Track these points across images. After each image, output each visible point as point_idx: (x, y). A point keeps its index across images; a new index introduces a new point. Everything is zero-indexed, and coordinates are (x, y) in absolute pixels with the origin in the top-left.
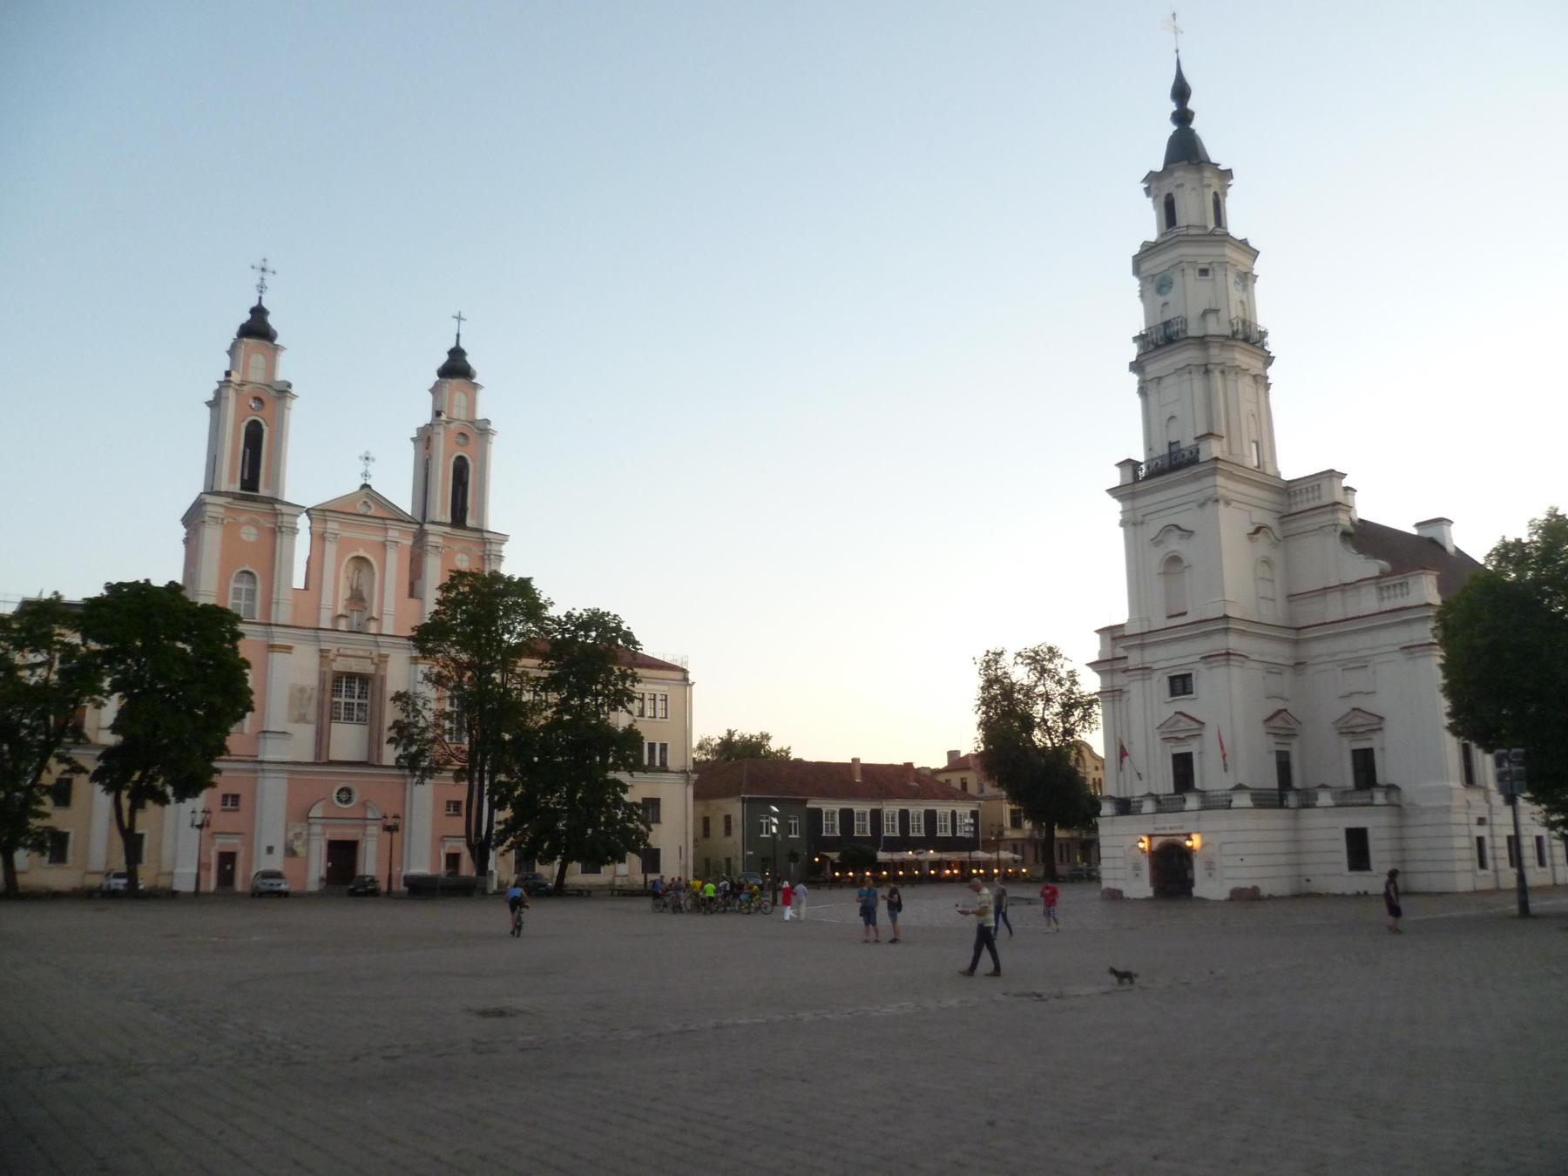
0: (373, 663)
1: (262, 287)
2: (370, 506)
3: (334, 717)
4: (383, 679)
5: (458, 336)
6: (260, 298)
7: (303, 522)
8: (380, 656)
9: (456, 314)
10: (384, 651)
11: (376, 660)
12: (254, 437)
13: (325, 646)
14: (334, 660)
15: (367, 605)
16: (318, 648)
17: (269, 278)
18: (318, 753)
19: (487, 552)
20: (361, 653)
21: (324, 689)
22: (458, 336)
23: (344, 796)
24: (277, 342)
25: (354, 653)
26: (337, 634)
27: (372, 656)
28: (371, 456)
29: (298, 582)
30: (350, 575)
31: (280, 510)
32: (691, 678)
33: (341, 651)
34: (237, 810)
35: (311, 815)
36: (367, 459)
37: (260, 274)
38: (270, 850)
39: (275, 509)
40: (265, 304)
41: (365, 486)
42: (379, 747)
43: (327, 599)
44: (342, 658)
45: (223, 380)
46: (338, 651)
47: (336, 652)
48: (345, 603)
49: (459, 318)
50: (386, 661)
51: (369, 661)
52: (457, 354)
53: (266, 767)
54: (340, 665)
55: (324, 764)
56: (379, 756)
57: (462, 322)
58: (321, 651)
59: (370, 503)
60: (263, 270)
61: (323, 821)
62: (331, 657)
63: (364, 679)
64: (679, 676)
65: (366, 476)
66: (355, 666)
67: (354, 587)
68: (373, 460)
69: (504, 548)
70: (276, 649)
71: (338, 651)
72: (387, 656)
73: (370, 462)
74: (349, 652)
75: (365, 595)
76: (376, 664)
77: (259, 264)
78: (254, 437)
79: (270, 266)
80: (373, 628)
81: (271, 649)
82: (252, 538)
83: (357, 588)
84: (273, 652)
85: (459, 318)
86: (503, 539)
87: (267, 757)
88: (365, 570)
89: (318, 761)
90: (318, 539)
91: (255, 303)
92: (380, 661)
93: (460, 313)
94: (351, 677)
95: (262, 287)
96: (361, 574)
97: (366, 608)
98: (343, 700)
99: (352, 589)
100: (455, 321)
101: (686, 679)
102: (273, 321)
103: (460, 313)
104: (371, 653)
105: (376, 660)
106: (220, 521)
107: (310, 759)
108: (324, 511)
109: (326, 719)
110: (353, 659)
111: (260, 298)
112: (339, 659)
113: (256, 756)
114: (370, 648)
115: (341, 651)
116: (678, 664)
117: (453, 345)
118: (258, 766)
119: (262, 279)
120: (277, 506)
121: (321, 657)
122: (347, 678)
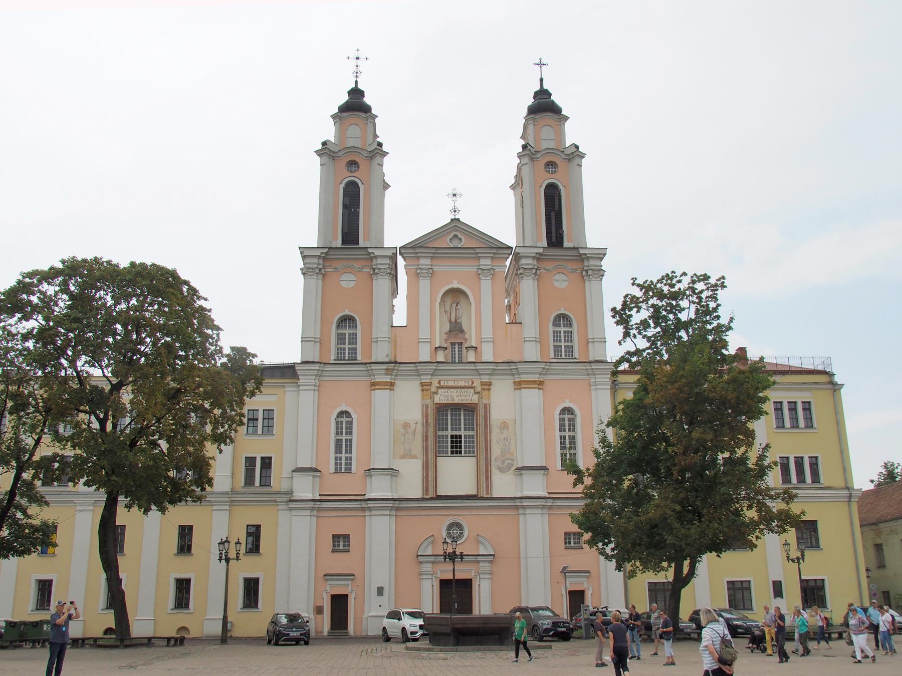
0: (476, 393)
1: (357, 73)
2: (460, 239)
3: (439, 452)
4: (486, 407)
5: (541, 80)
6: (356, 82)
8: (482, 384)
9: (538, 61)
10: (485, 379)
11: (479, 389)
12: (352, 195)
13: (426, 379)
14: (436, 393)
15: (467, 336)
16: (419, 382)
18: (426, 490)
20: (462, 384)
21: (427, 421)
22: (541, 80)
23: (455, 532)
24: (373, 112)
25: (456, 384)
26: (433, 367)
27: (473, 385)
28: (458, 192)
29: (400, 318)
30: (448, 308)
31: (374, 253)
32: (837, 379)
33: (442, 383)
34: (348, 551)
35: (419, 554)
36: (455, 195)
37: (355, 62)
38: (380, 591)
39: (369, 254)
40: (360, 87)
41: (455, 220)
42: (488, 478)
43: (424, 334)
44: (443, 390)
45: (320, 148)
46: (439, 383)
47: (438, 385)
48: (445, 336)
50: (489, 390)
51: (472, 390)
52: (542, 95)
53: (371, 504)
54: (442, 397)
55: (431, 499)
56: (489, 487)
57: (543, 67)
58: (422, 385)
59: (460, 236)
60: (358, 58)
61: (432, 559)
62: (433, 389)
63: (470, 409)
64: (823, 378)
65: (455, 211)
66: (457, 397)
67: (453, 320)
69: (602, 263)
70: (377, 387)
71: (439, 383)
72: (490, 384)
73: (458, 198)
74: (451, 383)
75: (464, 327)
76: (478, 393)
77: (353, 55)
78: (352, 195)
80: (471, 357)
81: (373, 388)
82: (352, 284)
83: (456, 320)
84: (375, 390)
85: (541, 64)
86: (601, 254)
87: (373, 495)
88: (463, 301)
89: (425, 497)
90: (415, 275)
92: (483, 389)
93: (540, 59)
94: (456, 408)
95: (357, 73)
96: (459, 307)
97: (466, 340)
98: (449, 433)
99: (450, 322)
100: (538, 67)
101: (832, 383)
102: (367, 100)
103: (540, 59)
104: (473, 383)
105: (479, 389)
106: (317, 271)
107: (419, 495)
109: (431, 455)
110: (454, 390)
111: (356, 82)
112: (440, 391)
113: (365, 495)
114: (471, 377)
115: (442, 383)
116: (820, 368)
117: (538, 88)
118: (364, 505)
119: (357, 66)
120: (370, 251)
121: (423, 390)
122: (452, 410)
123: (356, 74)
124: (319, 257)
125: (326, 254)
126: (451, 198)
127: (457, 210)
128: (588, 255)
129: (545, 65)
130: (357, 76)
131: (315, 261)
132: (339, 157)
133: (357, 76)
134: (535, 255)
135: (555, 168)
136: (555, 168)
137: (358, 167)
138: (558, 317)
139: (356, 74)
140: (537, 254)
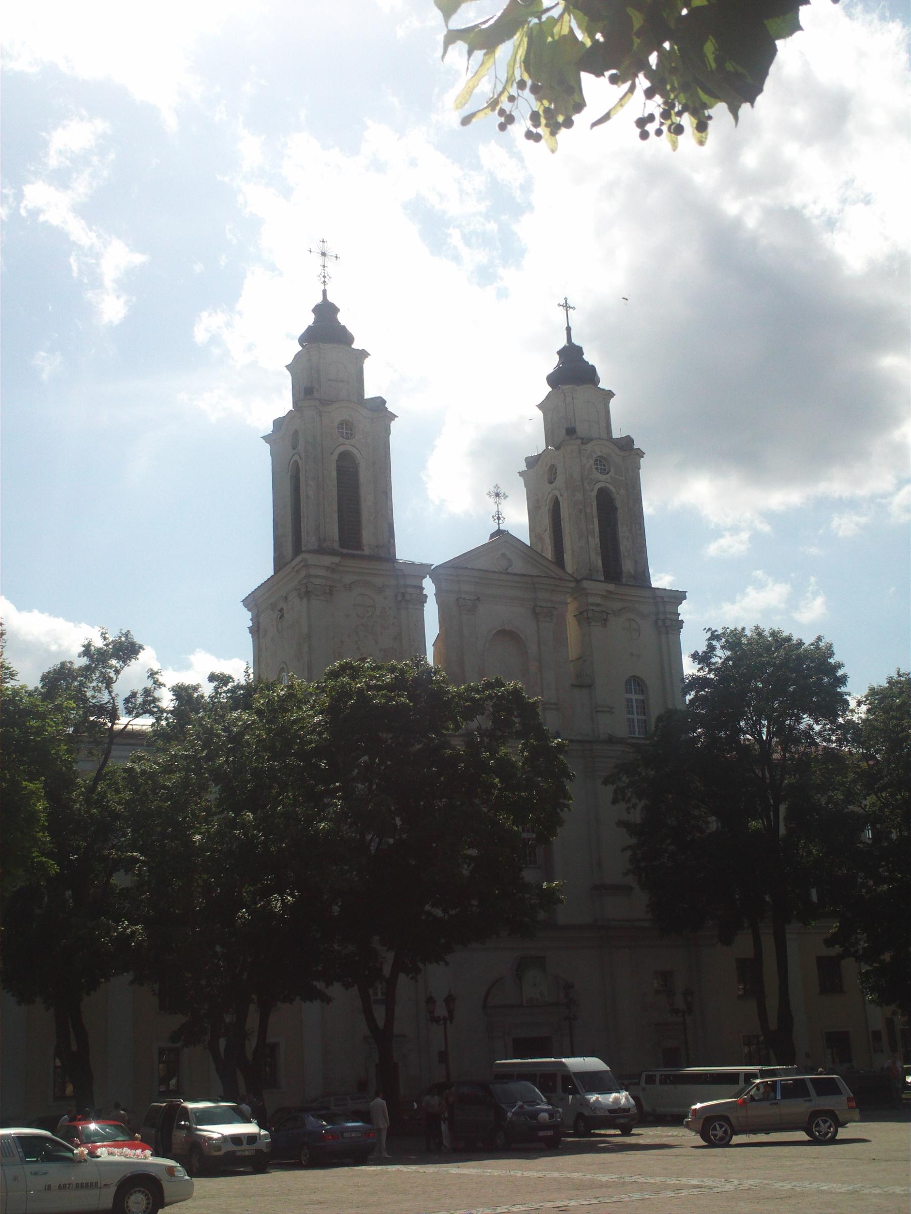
1: (324, 277)
5: (569, 329)
6: (324, 292)
7: (429, 587)
17: (332, 267)
19: (661, 616)
22: (569, 329)
28: (502, 491)
49: (567, 307)
60: (324, 254)
68: (505, 497)
79: (331, 249)
86: (679, 597)
91: (319, 299)
93: (566, 299)
103: (566, 299)
108: (457, 568)
111: (324, 292)
119: (324, 266)
123: (323, 279)
124: (327, 568)
125: (337, 564)
126: (492, 500)
127: (500, 516)
128: (665, 600)
129: (566, 301)
130: (324, 282)
131: (322, 572)
132: (330, 412)
133: (324, 282)
134: (604, 593)
135: (604, 465)
136: (604, 465)
137: (351, 430)
138: (628, 682)
139: (323, 279)
140: (607, 591)
